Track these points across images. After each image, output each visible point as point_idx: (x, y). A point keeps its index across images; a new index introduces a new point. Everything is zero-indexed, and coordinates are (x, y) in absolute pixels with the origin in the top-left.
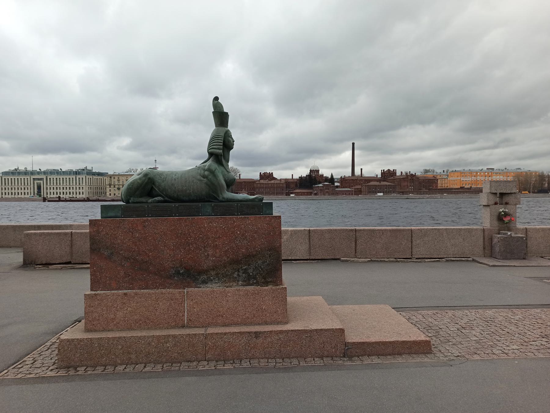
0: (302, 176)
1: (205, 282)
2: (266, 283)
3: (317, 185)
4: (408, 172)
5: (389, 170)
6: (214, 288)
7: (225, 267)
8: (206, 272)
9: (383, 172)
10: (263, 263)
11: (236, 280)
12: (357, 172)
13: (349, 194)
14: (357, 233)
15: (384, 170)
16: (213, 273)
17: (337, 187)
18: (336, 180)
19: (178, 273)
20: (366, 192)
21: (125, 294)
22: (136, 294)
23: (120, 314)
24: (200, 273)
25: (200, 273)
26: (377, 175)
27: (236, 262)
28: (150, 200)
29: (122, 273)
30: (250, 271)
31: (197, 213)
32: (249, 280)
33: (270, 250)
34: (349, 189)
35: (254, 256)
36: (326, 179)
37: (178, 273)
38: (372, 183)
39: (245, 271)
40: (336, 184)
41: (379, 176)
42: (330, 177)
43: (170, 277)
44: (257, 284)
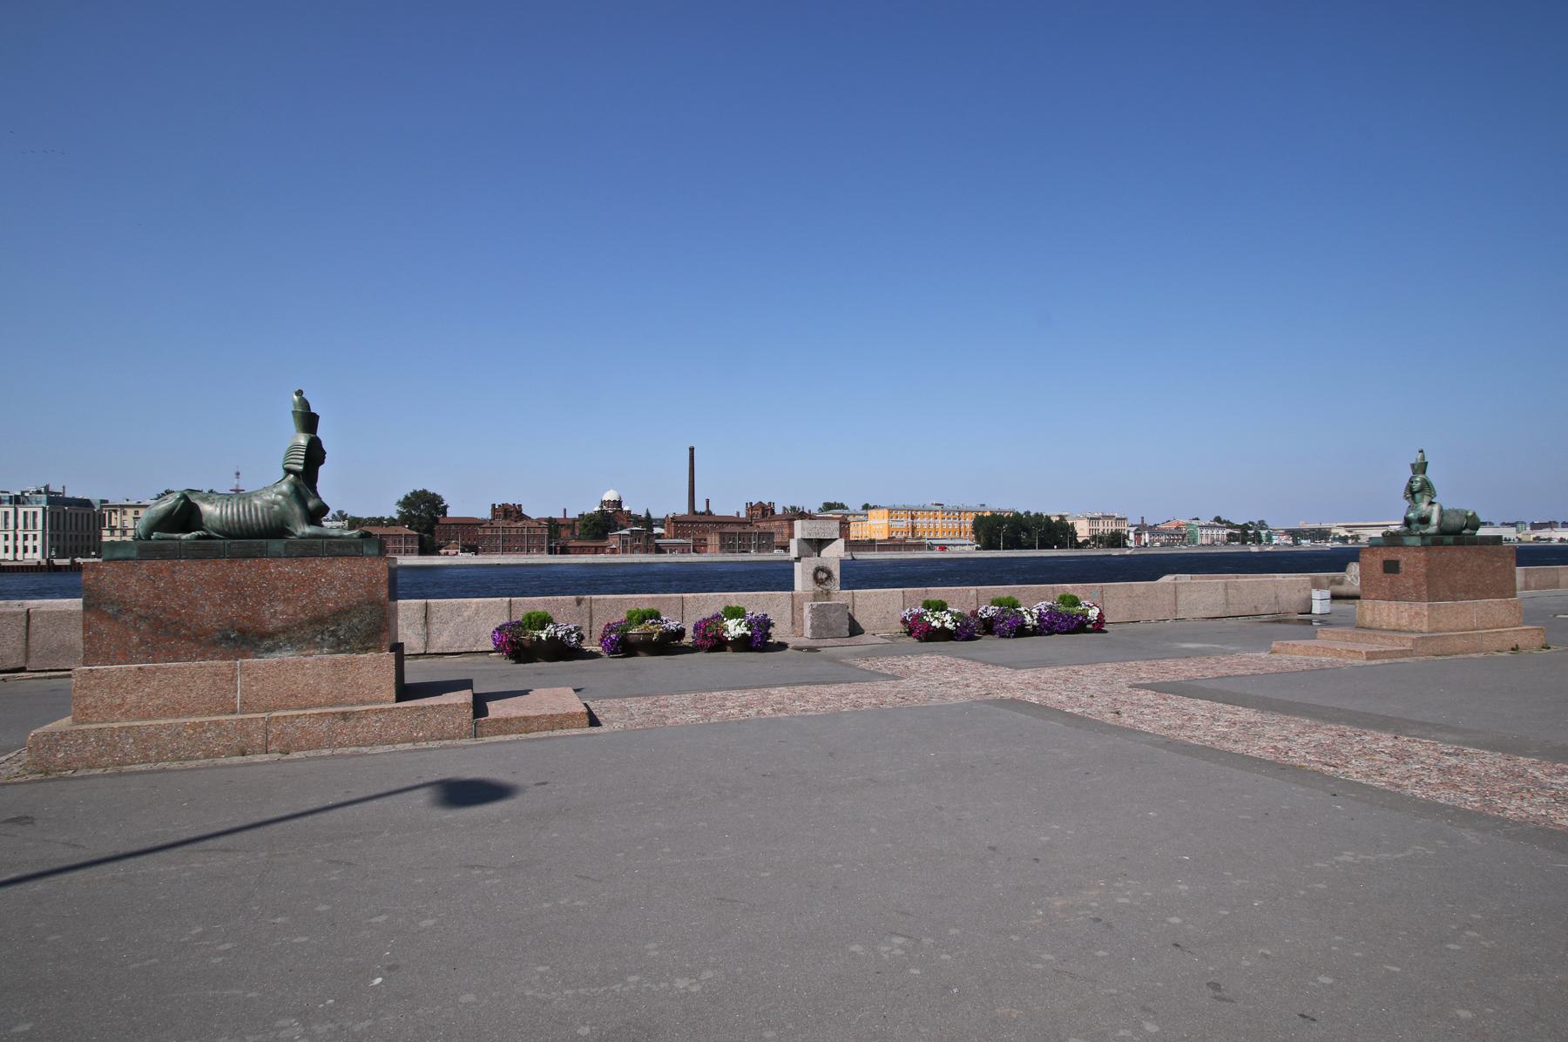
0: (585, 514)
1: (270, 650)
2: (367, 650)
3: (617, 531)
5: (761, 502)
6: (287, 656)
7: (301, 628)
8: (271, 635)
10: (361, 621)
11: (319, 646)
12: (700, 507)
14: (593, 604)
15: (751, 503)
17: (659, 536)
18: (656, 520)
19: (227, 638)
20: (718, 547)
21: (140, 668)
22: (158, 669)
23: (131, 698)
24: (264, 636)
25: (264, 636)
26: (738, 513)
27: (318, 620)
28: (184, 536)
29: (135, 639)
30: (341, 633)
31: (263, 553)
32: (339, 646)
33: (371, 604)
34: (682, 541)
35: (347, 612)
36: (637, 520)
37: (227, 638)
38: (728, 529)
39: (333, 633)
40: (657, 530)
41: (743, 515)
42: (643, 516)
43: (215, 643)
44: (352, 651)
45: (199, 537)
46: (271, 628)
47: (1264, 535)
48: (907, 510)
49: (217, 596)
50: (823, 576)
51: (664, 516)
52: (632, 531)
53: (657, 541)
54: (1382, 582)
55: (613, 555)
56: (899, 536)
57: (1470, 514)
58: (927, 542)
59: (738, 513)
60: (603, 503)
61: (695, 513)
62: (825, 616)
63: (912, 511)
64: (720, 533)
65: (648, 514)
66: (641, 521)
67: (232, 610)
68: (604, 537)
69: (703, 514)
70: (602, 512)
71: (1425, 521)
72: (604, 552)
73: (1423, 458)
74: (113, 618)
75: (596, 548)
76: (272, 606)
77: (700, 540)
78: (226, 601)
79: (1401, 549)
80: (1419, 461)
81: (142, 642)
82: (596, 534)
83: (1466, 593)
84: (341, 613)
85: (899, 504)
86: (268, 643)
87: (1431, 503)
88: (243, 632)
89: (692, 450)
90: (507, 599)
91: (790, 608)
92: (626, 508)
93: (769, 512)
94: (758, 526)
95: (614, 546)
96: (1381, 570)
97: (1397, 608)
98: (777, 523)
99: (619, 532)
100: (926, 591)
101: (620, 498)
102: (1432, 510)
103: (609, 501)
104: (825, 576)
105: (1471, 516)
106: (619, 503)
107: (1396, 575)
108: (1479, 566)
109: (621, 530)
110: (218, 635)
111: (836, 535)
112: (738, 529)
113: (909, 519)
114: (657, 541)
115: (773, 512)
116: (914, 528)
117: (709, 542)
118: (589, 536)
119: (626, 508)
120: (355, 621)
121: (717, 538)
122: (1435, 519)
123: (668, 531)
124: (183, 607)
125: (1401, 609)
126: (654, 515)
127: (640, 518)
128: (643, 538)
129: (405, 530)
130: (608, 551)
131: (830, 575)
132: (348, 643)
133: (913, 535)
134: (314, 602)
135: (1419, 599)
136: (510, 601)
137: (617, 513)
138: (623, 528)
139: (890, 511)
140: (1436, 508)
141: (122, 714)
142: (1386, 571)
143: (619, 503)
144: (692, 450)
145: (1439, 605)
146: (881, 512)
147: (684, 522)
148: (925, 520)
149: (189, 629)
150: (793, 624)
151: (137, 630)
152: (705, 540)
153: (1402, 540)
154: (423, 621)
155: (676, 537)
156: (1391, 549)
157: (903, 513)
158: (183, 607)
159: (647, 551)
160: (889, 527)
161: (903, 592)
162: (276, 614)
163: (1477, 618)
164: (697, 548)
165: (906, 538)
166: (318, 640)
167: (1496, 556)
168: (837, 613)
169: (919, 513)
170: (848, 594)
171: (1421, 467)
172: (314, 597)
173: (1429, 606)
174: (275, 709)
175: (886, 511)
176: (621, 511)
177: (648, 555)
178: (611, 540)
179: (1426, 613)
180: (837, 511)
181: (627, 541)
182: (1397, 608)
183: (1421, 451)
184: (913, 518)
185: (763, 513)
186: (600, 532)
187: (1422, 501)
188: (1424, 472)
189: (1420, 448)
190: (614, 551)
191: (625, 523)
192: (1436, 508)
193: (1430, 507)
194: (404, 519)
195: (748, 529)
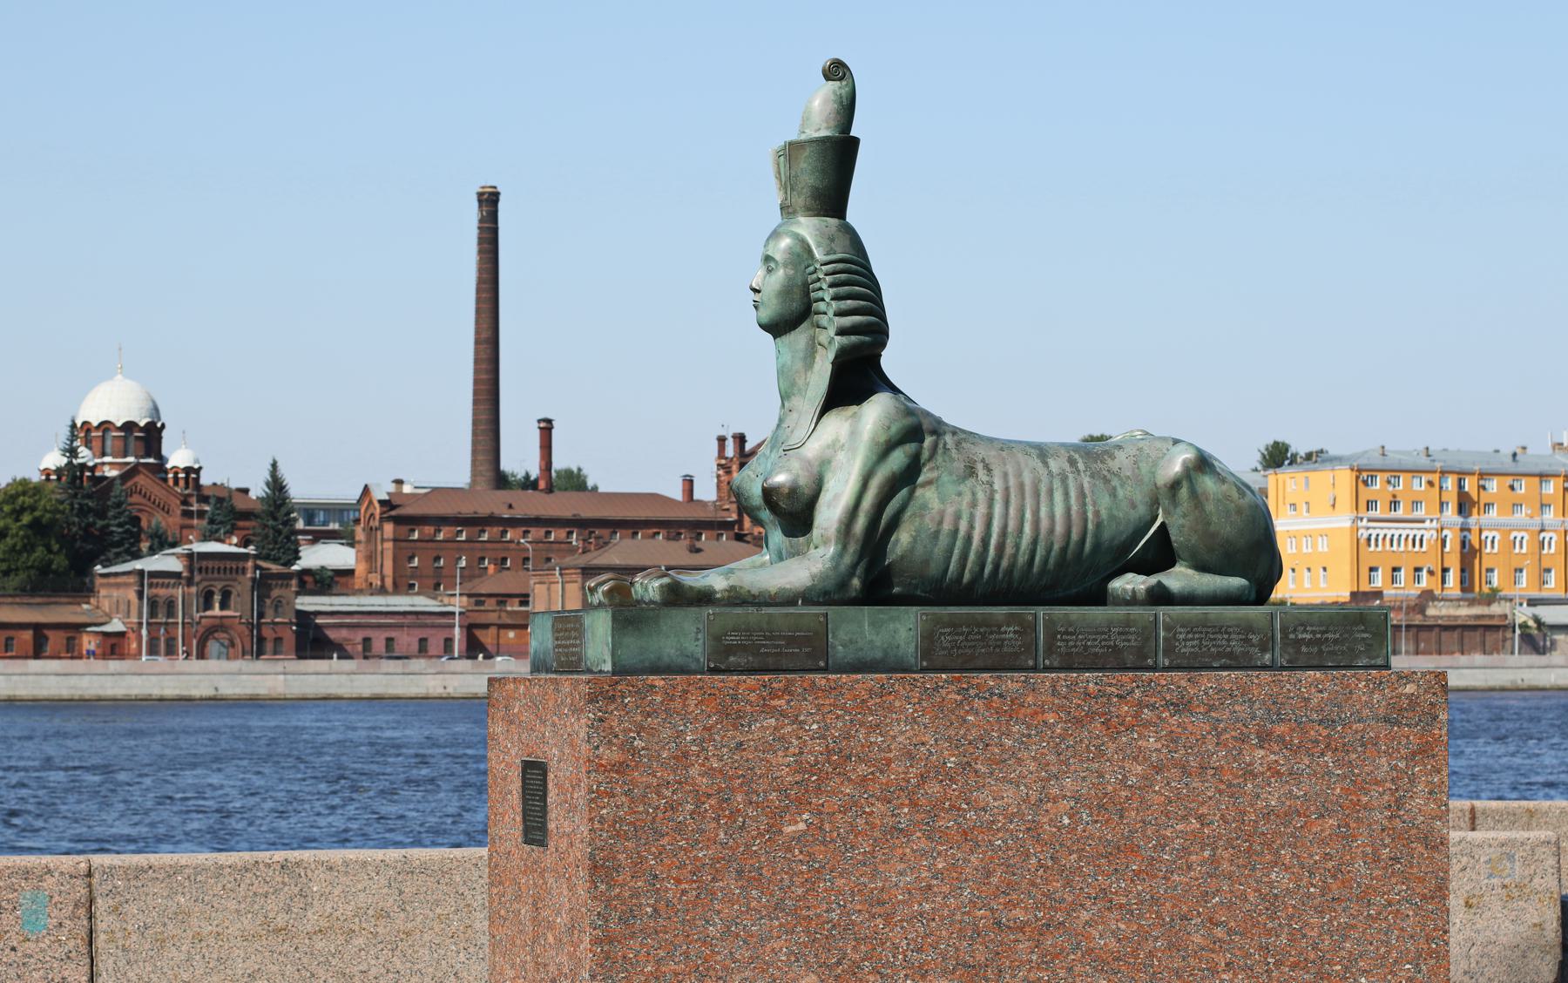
0: (18, 479)
3: (137, 556)
9: (730, 451)
12: (519, 457)
13: (423, 649)
15: (741, 439)
17: (325, 581)
18: (310, 512)
26: (689, 483)
40: (316, 556)
41: (706, 491)
42: (258, 490)
47: (171, 591)
48: (1435, 470)
51: (352, 494)
52: (190, 556)
53: (307, 603)
55: (114, 665)
56: (1405, 589)
58: (1523, 615)
59: (689, 483)
60: (82, 432)
61: (501, 481)
63: (1461, 475)
65: (277, 485)
66: (247, 515)
68: (76, 583)
69: (528, 484)
70: (73, 475)
72: (72, 651)
73: (847, 109)
75: (38, 628)
77: (502, 599)
82: (44, 569)
85: (1405, 443)
89: (489, 201)
92: (177, 457)
95: (116, 626)
99: (138, 565)
101: (156, 410)
103: (105, 426)
106: (149, 436)
108: (1104, 806)
109: (153, 551)
113: (1450, 514)
114: (307, 603)
116: (1469, 553)
117: (538, 604)
118: (14, 581)
119: (177, 457)
123: (370, 558)
126: (300, 491)
127: (240, 504)
128: (242, 587)
130: (88, 642)
133: (1466, 584)
137: (141, 480)
138: (161, 543)
139: (1364, 475)
143: (149, 436)
144: (489, 201)
146: (1320, 478)
147: (441, 521)
148: (1521, 516)
152: (524, 599)
155: (402, 585)
157: (1419, 485)
159: (258, 648)
160: (1359, 546)
164: (487, 637)
165: (1428, 596)
167: (1264, 738)
169: (1493, 485)
175: (1345, 478)
176: (160, 469)
177: (259, 665)
178: (106, 597)
181: (170, 605)
184: (1465, 505)
186: (60, 561)
189: (824, 60)
190: (114, 646)
191: (170, 522)
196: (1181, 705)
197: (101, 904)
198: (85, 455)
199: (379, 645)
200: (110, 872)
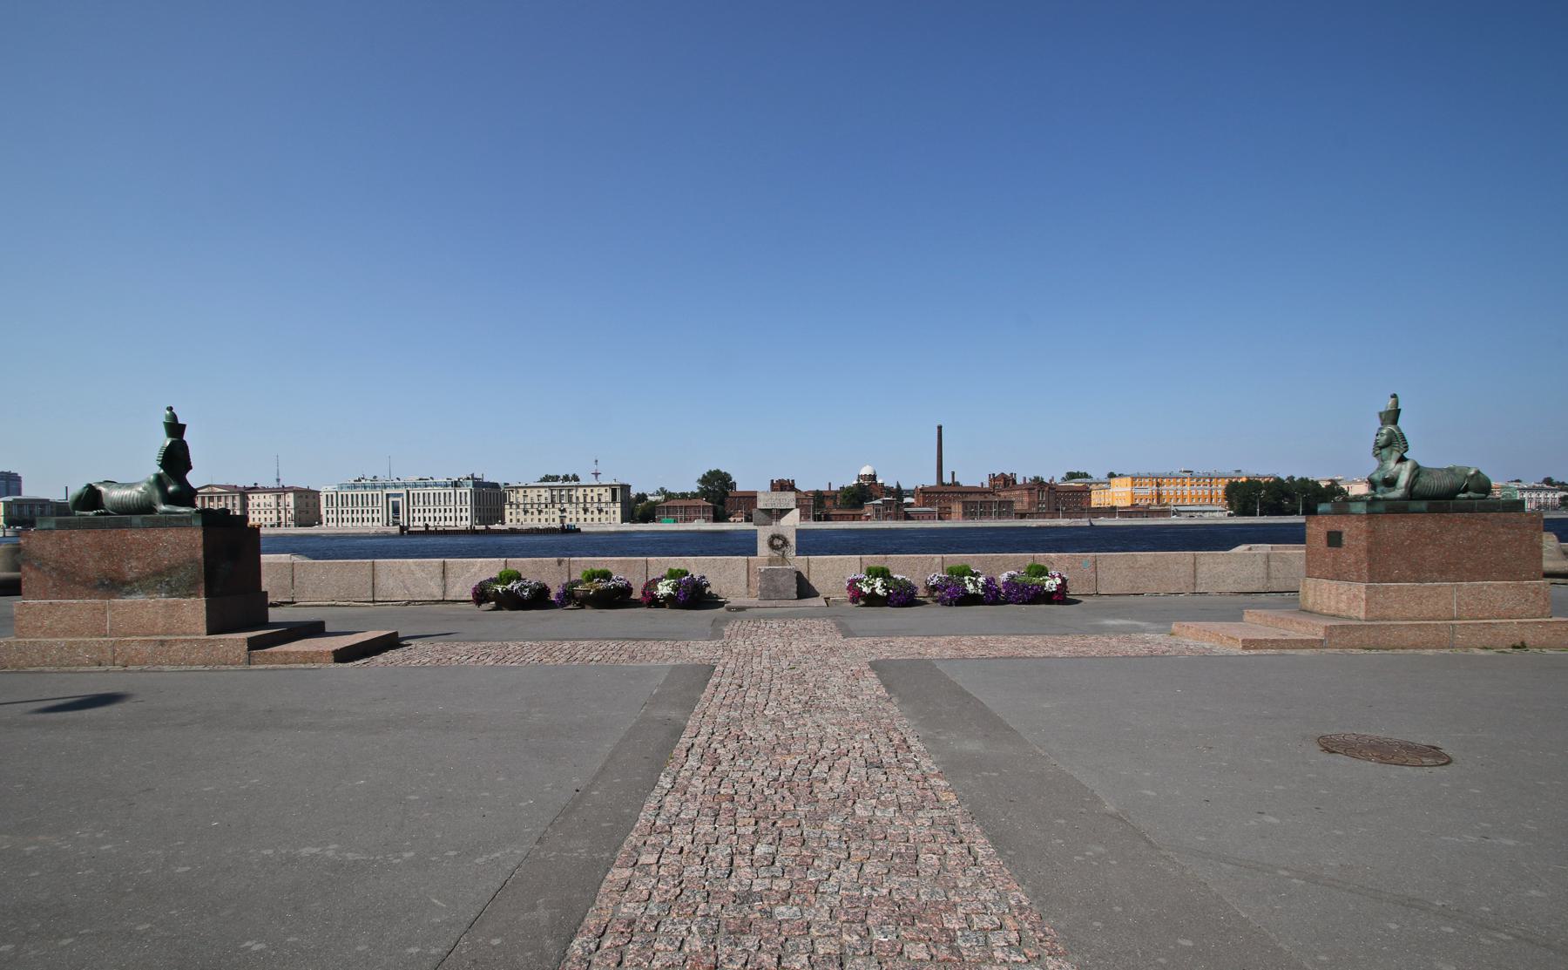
0: (845, 486)
1: (129, 593)
2: (190, 595)
4: (733, 480)
5: (1003, 474)
6: (139, 599)
8: (130, 583)
10: (185, 575)
11: (158, 592)
12: (947, 479)
13: (929, 518)
15: (994, 475)
16: (136, 584)
17: (909, 505)
19: (103, 584)
20: (961, 515)
21: (51, 603)
22: (61, 604)
23: (47, 622)
24: (124, 583)
25: (124, 583)
26: (982, 484)
27: (159, 573)
28: (91, 513)
29: (51, 584)
31: (129, 525)
32: (172, 592)
34: (929, 509)
35: (176, 568)
36: (889, 491)
37: (103, 584)
39: (168, 583)
40: (907, 500)
41: (987, 485)
42: (895, 487)
43: (96, 588)
44: (180, 596)
45: (97, 514)
46: (129, 578)
48: (1151, 477)
49: (97, 555)
50: (778, 542)
51: (913, 488)
53: (906, 509)
54: (1325, 557)
56: (1143, 503)
57: (1472, 472)
58: (1173, 508)
59: (982, 484)
61: (943, 484)
62: (772, 580)
63: (1157, 478)
64: (963, 502)
65: (898, 486)
67: (105, 565)
68: (862, 507)
69: (948, 485)
70: (859, 485)
71: (1391, 483)
72: (860, 519)
74: (38, 569)
76: (129, 563)
77: (945, 508)
78: (102, 558)
79: (1344, 518)
80: (1389, 409)
81: (55, 585)
82: (854, 504)
83: (1442, 573)
84: (171, 569)
85: (1143, 472)
86: (127, 588)
87: (1402, 459)
88: (112, 580)
89: (940, 428)
90: (505, 559)
91: (746, 572)
92: (879, 481)
93: (1011, 483)
94: (999, 496)
95: (868, 514)
96: (1325, 544)
97: (1337, 589)
98: (1017, 492)
100: (886, 558)
102: (1401, 469)
104: (781, 542)
105: (1473, 476)
106: (873, 477)
107: (1339, 549)
110: (98, 582)
111: (793, 505)
112: (979, 498)
113: (1154, 487)
114: (906, 509)
115: (1014, 482)
116: (1159, 495)
117: (953, 510)
118: (849, 506)
119: (879, 481)
120: (182, 574)
121: (960, 506)
122: (1403, 479)
123: (918, 500)
124: (77, 562)
125: (1341, 591)
126: (904, 487)
129: (702, 502)
130: (863, 518)
131: (786, 543)
132: (177, 590)
133: (1158, 502)
134: (155, 560)
135: (1359, 579)
136: (506, 561)
138: (877, 498)
139: (1134, 478)
140: (1408, 466)
141: (42, 633)
142: (1330, 544)
143: (873, 477)
144: (940, 428)
145: (1387, 587)
146: (1124, 480)
147: (931, 493)
148: (1172, 486)
149: (80, 577)
150: (748, 586)
151: (51, 577)
152: (950, 508)
153: (1349, 506)
154: (442, 575)
155: (924, 506)
156: (1335, 517)
157: (1147, 481)
158: (77, 562)
159: (897, 518)
160: (1133, 494)
161: (861, 559)
162: (132, 569)
163: (1458, 604)
164: (942, 516)
165: (1149, 505)
166: (158, 587)
167: (1503, 526)
168: (785, 577)
169: (1165, 480)
170: (803, 559)
171: (1393, 416)
172: (155, 556)
173: (1367, 588)
174: (130, 635)
175: (1129, 479)
176: (876, 483)
178: (866, 509)
179: (1364, 596)
180: (1079, 480)
181: (879, 511)
182: (1337, 589)
183: (1394, 396)
184: (1158, 485)
185: (1005, 483)
187: (1389, 458)
188: (1395, 422)
190: (868, 518)
191: (878, 494)
192: (1408, 466)
193: (1399, 466)
194: (703, 493)
195: (990, 498)
196: (1485, 520)
197: (1098, 562)
198: (861, 481)
199: (921, 518)
200: (1100, 556)
